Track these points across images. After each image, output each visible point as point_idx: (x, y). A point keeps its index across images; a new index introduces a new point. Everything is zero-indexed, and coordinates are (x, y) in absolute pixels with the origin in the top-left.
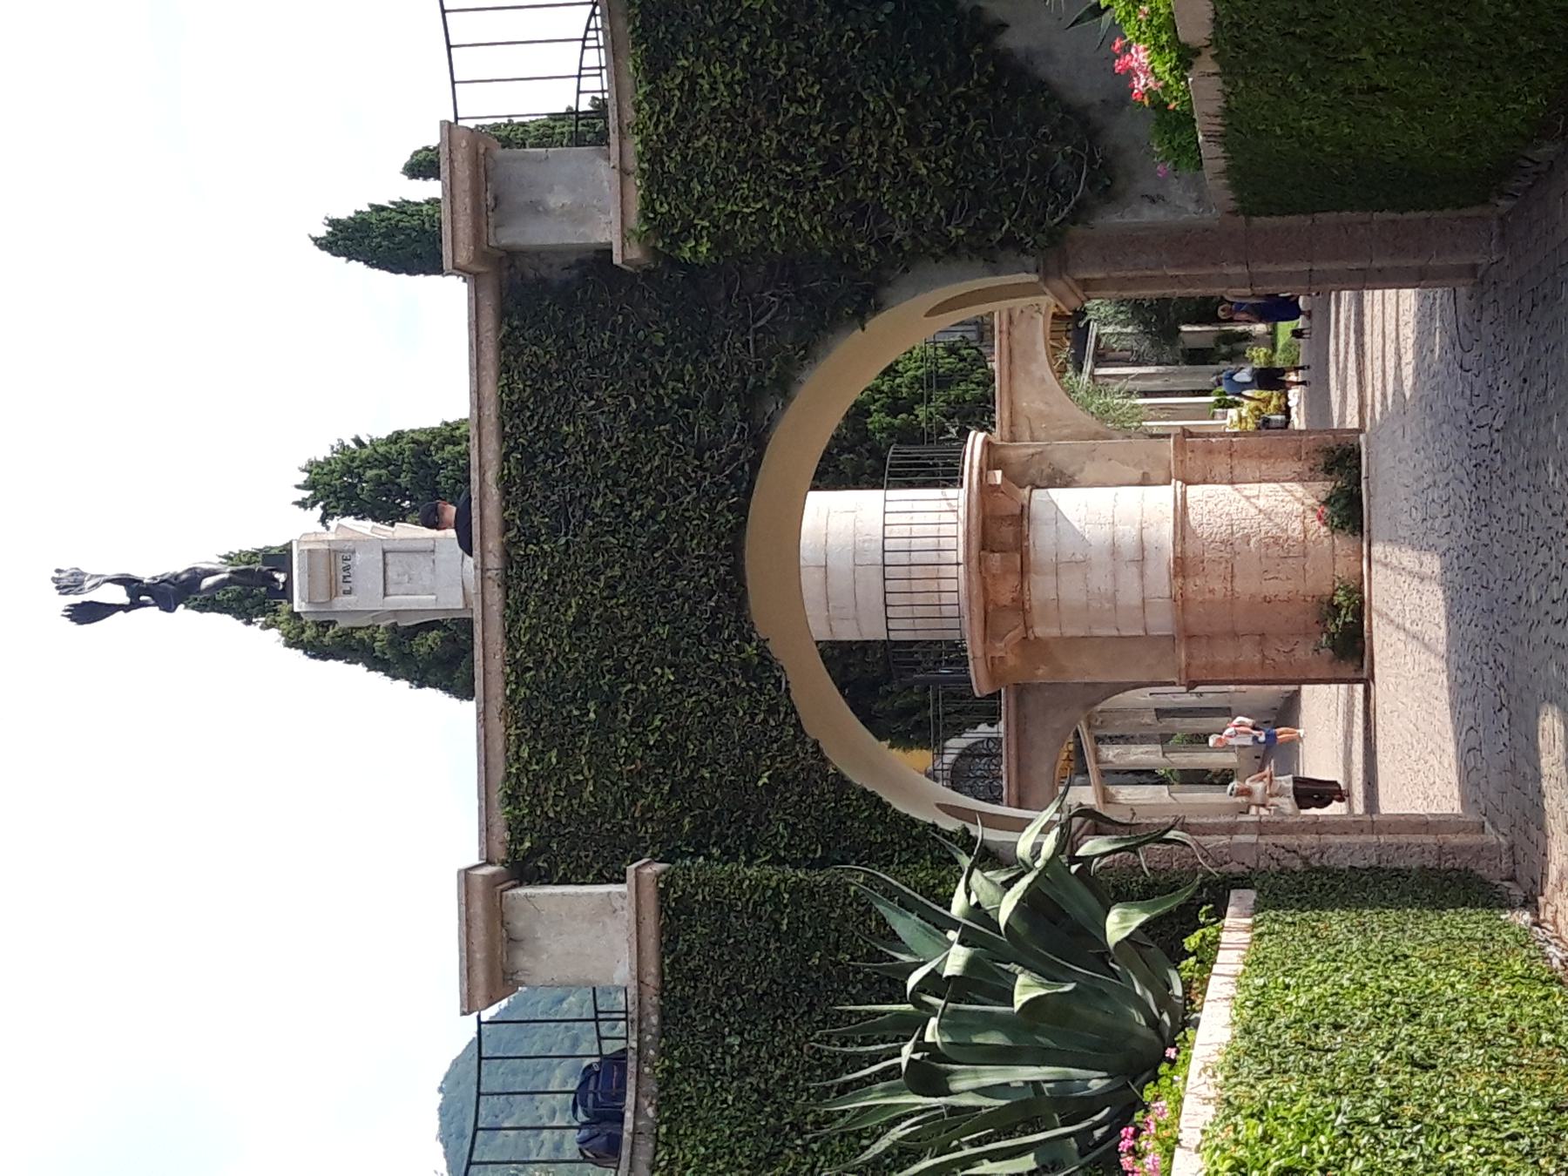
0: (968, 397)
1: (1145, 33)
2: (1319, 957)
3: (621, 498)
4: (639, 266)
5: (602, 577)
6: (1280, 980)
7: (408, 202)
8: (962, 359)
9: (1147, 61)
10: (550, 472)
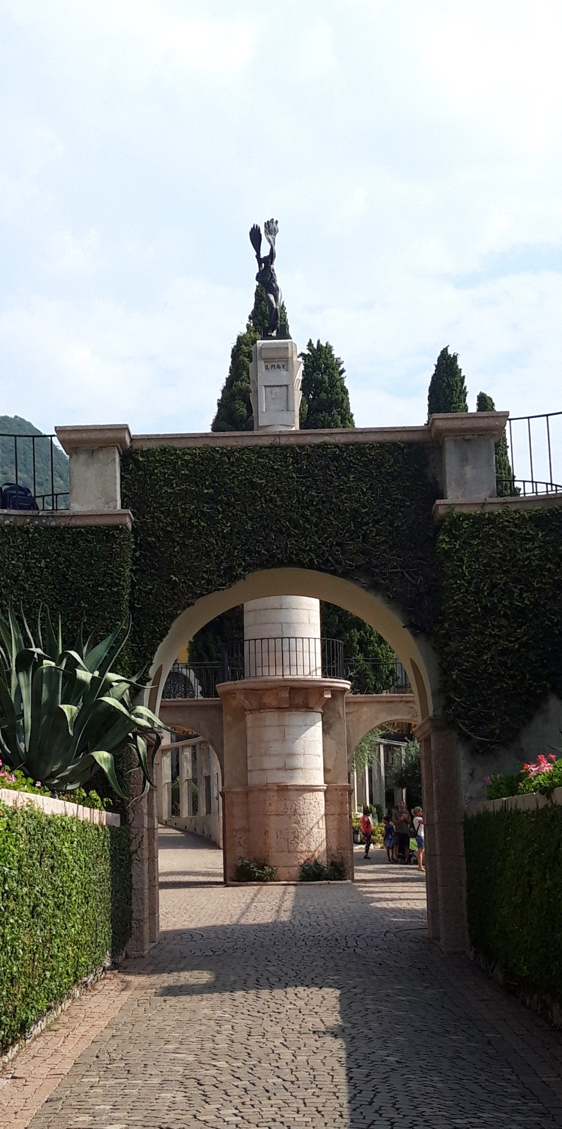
0: (368, 680)
1: (559, 770)
2: (87, 859)
3: (316, 505)
4: (435, 513)
5: (276, 496)
6: (76, 839)
7: (466, 396)
8: (387, 677)
9: (544, 771)
10: (329, 469)
